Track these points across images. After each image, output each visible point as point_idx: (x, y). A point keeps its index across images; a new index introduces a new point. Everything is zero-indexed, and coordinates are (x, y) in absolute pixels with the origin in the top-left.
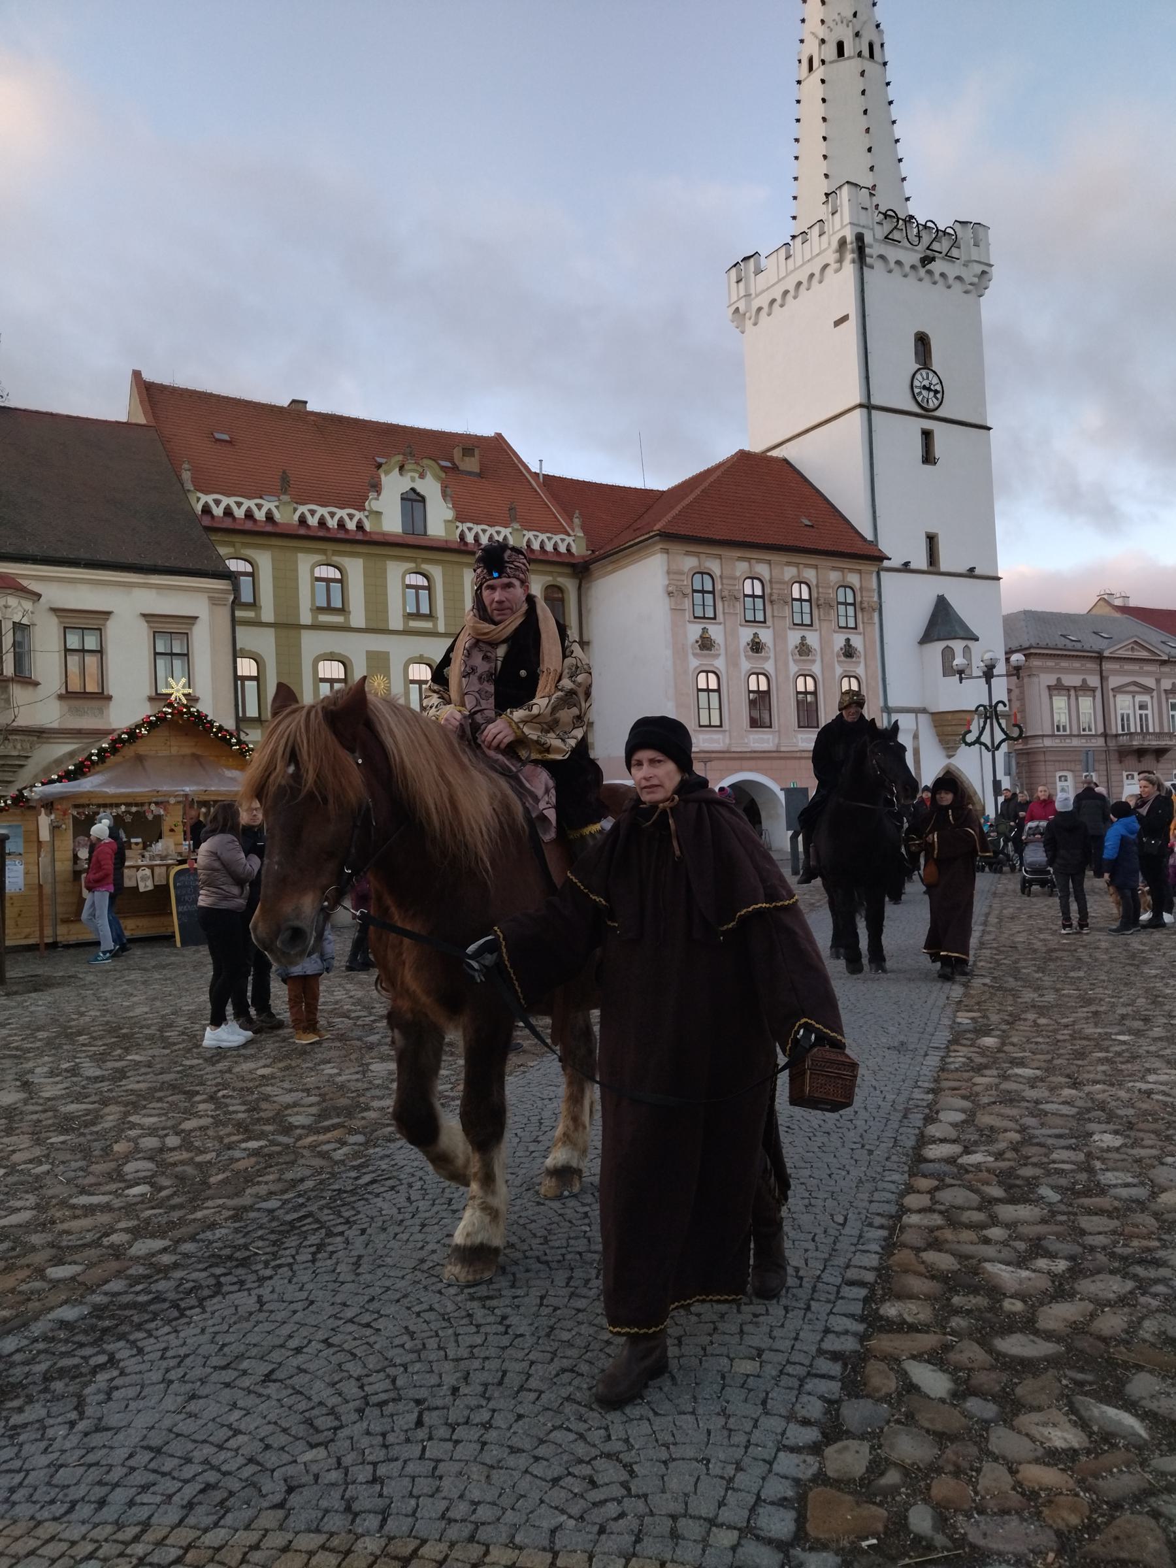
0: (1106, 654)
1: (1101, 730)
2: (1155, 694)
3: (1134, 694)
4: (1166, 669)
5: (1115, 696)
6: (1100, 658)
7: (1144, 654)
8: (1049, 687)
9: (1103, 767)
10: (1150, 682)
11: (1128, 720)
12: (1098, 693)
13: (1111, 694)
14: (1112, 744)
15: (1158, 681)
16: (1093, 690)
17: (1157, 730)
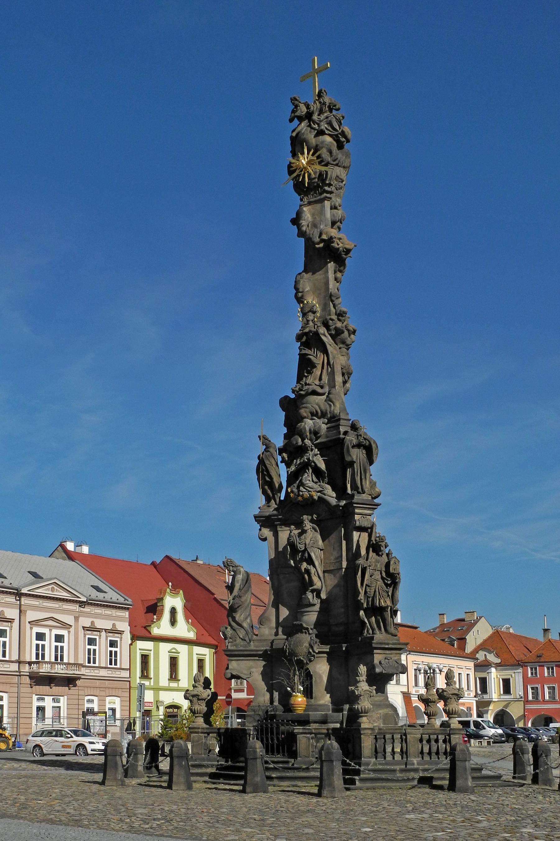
0: (24, 591)
1: (15, 657)
2: (72, 630)
3: (51, 627)
4: (87, 609)
5: (31, 628)
6: (19, 595)
7: (64, 595)
9: (16, 690)
10: (69, 619)
11: (62, 651)
12: (16, 624)
13: (28, 626)
14: (26, 669)
15: (76, 619)
16: (11, 621)
17: (72, 661)
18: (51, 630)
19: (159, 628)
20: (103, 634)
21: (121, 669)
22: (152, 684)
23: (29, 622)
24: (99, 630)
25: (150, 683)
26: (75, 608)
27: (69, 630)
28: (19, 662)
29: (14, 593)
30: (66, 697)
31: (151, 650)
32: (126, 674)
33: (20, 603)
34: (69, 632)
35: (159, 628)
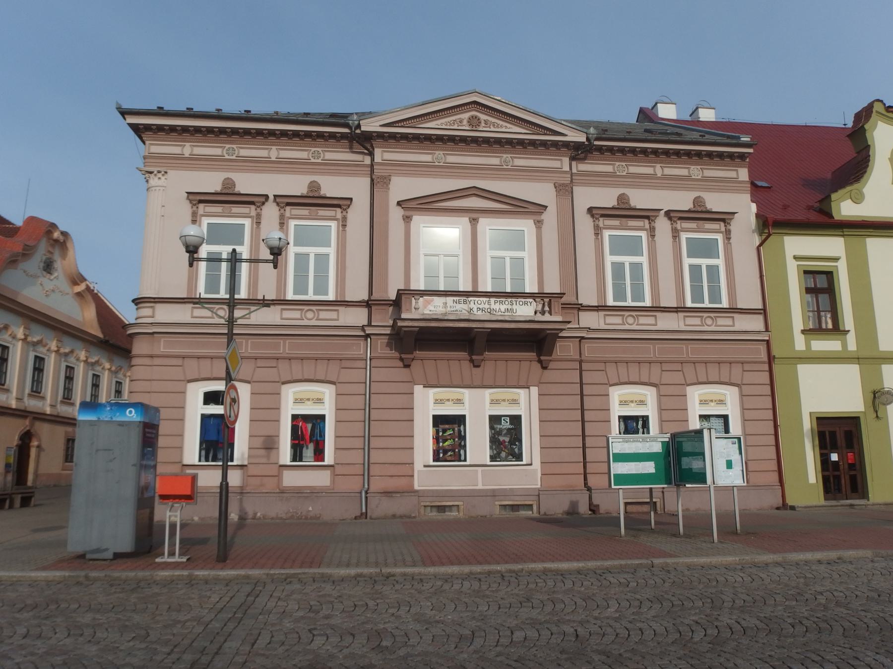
2: (550, 217)
5: (407, 219)
8: (198, 199)
12: (358, 215)
13: (396, 214)
15: (565, 190)
16: (342, 204)
18: (474, 222)
19: (858, 199)
20: (663, 225)
21: (733, 310)
22: (852, 345)
23: (399, 203)
24: (648, 215)
25: (844, 345)
26: (555, 164)
27: (537, 218)
28: (368, 304)
29: (343, 136)
30: (534, 390)
31: (836, 259)
32: (755, 323)
33: (372, 160)
34: (539, 224)
35: (858, 199)
